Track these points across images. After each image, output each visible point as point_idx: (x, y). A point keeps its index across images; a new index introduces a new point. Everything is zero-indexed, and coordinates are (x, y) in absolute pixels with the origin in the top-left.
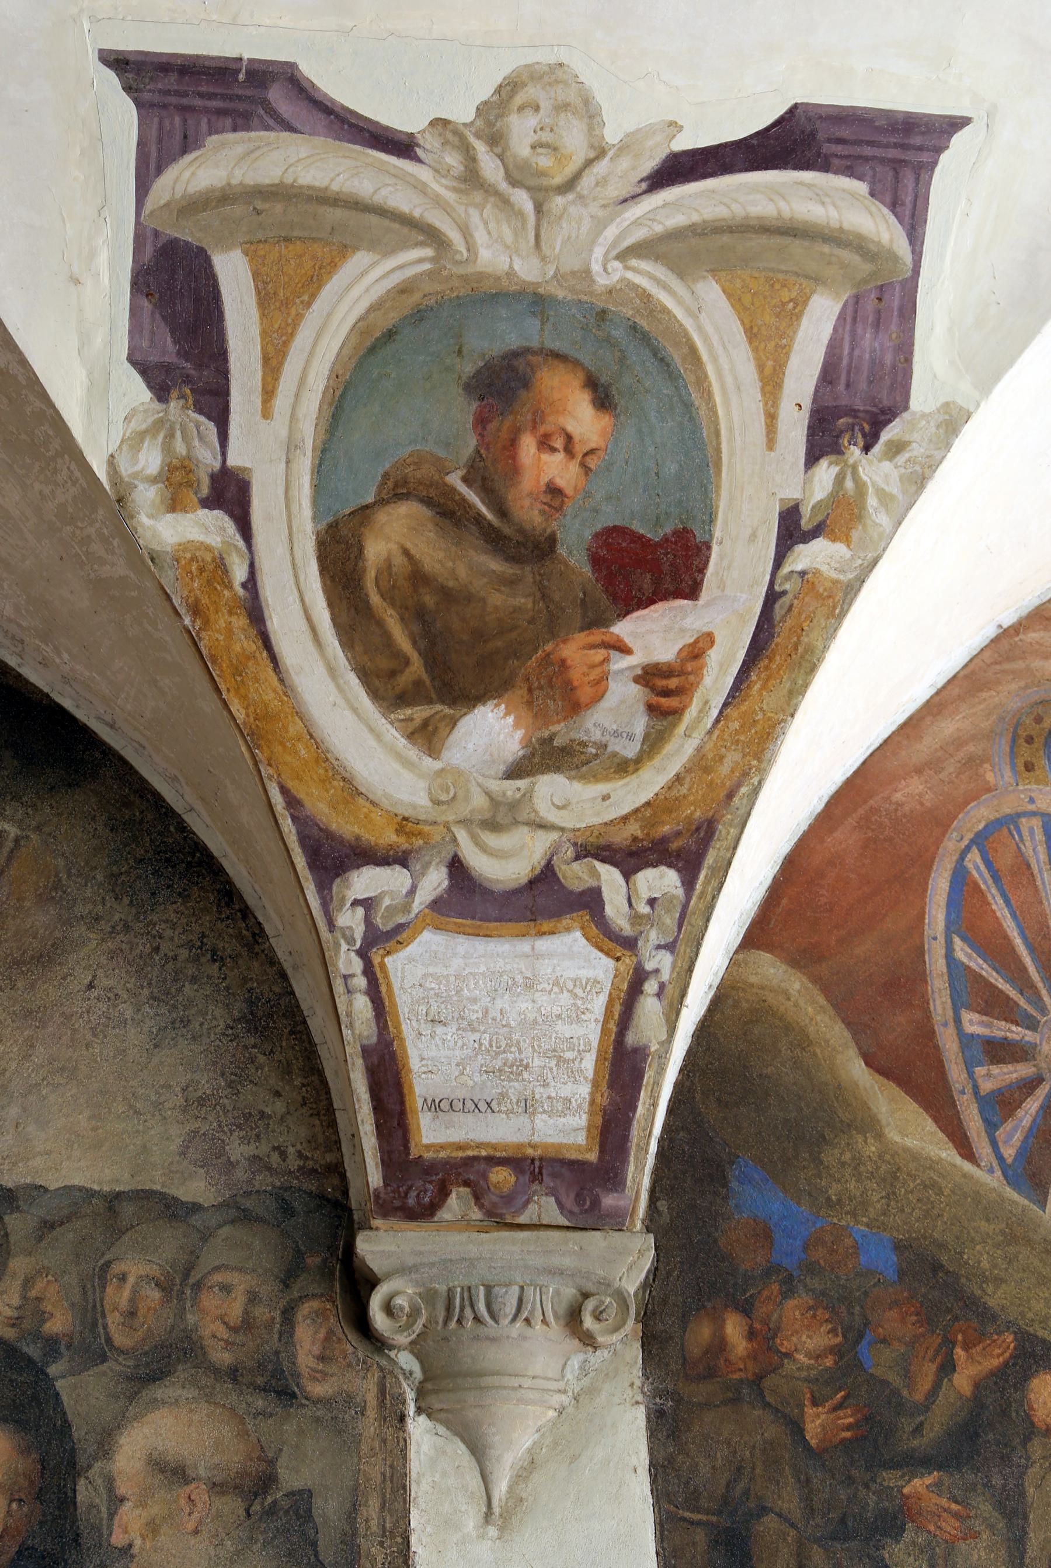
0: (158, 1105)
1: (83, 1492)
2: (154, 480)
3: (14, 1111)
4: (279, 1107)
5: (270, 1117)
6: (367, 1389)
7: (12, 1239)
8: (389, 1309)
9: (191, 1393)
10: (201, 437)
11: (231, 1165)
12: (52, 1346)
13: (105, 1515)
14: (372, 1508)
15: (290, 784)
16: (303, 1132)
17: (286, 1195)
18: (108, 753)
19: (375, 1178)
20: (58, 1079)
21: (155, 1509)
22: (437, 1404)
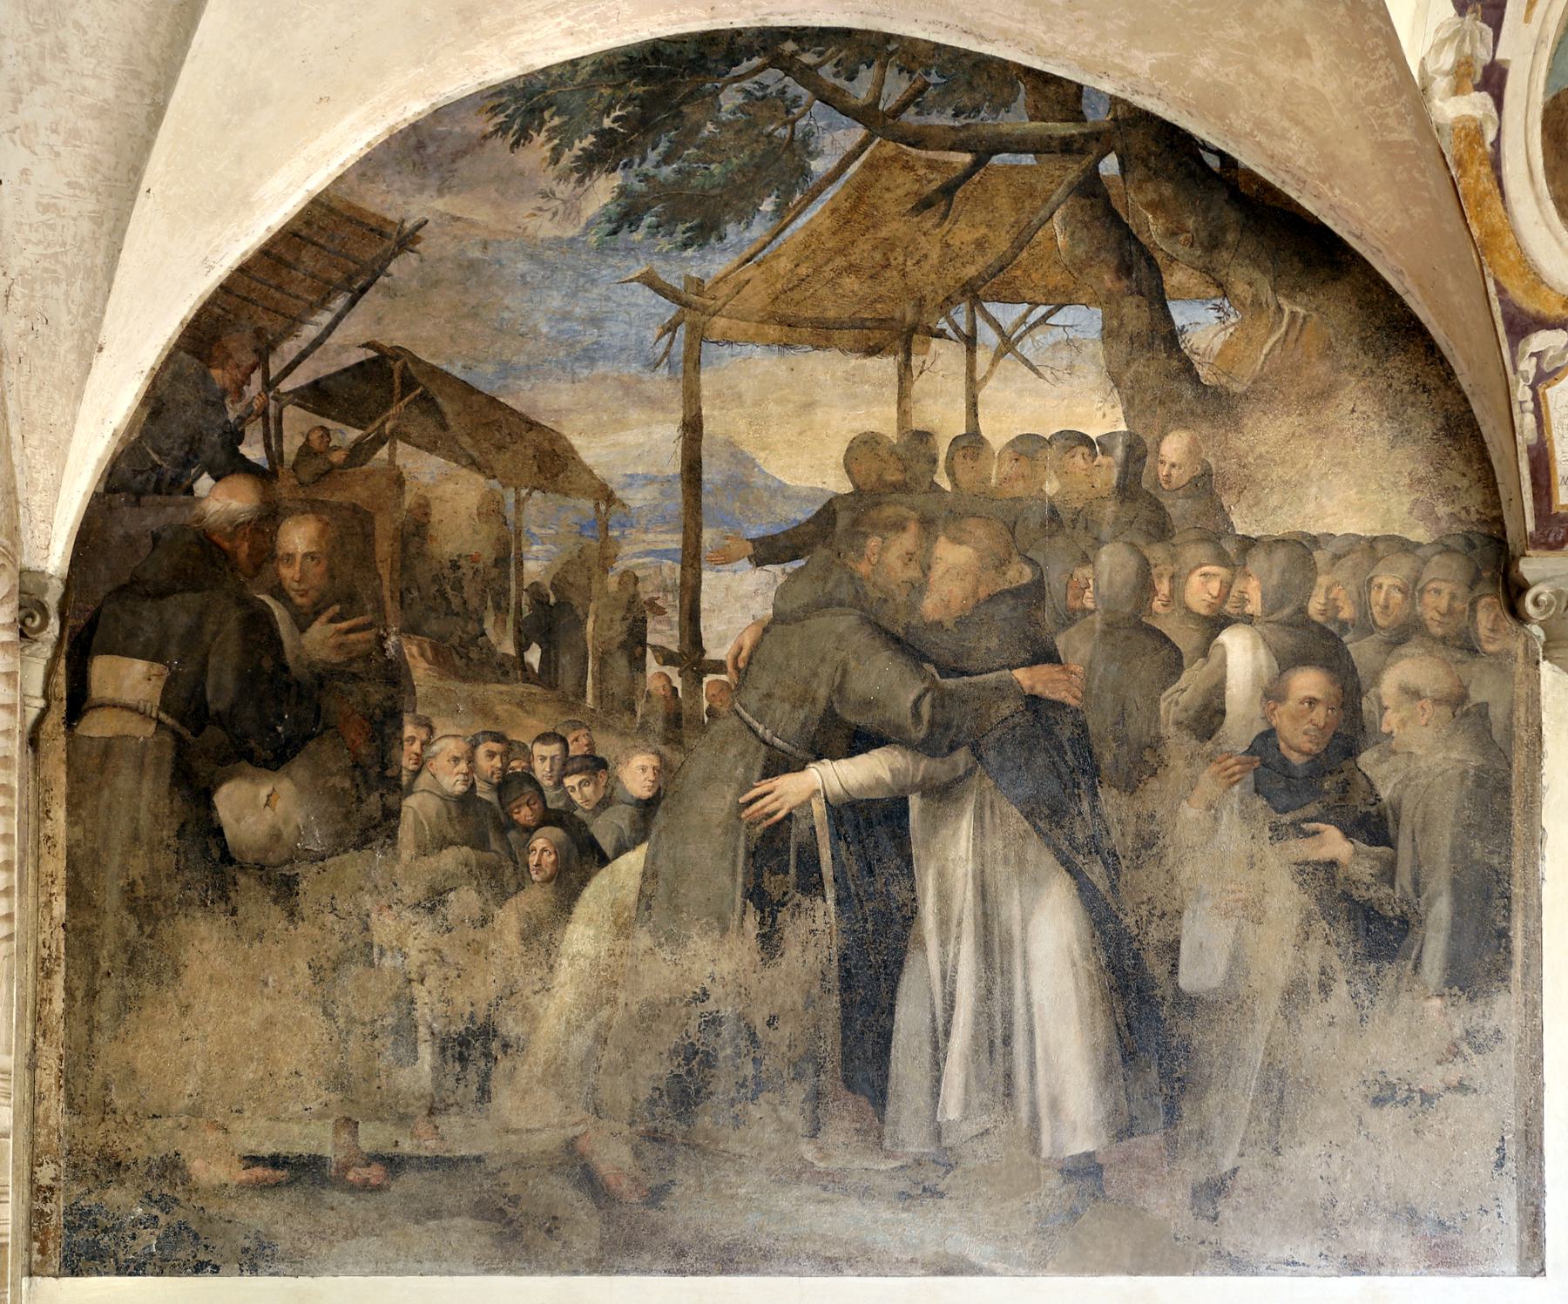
0: (1395, 484)
1: (1365, 705)
2: (1447, 74)
3: (1314, 490)
4: (1465, 483)
6: (1518, 647)
8: (1536, 602)
9: (1421, 651)
10: (1482, 40)
12: (1344, 625)
14: (1521, 712)
16: (1480, 498)
19: (1530, 526)
20: (1337, 470)
21: (1404, 713)
22: (1556, 654)
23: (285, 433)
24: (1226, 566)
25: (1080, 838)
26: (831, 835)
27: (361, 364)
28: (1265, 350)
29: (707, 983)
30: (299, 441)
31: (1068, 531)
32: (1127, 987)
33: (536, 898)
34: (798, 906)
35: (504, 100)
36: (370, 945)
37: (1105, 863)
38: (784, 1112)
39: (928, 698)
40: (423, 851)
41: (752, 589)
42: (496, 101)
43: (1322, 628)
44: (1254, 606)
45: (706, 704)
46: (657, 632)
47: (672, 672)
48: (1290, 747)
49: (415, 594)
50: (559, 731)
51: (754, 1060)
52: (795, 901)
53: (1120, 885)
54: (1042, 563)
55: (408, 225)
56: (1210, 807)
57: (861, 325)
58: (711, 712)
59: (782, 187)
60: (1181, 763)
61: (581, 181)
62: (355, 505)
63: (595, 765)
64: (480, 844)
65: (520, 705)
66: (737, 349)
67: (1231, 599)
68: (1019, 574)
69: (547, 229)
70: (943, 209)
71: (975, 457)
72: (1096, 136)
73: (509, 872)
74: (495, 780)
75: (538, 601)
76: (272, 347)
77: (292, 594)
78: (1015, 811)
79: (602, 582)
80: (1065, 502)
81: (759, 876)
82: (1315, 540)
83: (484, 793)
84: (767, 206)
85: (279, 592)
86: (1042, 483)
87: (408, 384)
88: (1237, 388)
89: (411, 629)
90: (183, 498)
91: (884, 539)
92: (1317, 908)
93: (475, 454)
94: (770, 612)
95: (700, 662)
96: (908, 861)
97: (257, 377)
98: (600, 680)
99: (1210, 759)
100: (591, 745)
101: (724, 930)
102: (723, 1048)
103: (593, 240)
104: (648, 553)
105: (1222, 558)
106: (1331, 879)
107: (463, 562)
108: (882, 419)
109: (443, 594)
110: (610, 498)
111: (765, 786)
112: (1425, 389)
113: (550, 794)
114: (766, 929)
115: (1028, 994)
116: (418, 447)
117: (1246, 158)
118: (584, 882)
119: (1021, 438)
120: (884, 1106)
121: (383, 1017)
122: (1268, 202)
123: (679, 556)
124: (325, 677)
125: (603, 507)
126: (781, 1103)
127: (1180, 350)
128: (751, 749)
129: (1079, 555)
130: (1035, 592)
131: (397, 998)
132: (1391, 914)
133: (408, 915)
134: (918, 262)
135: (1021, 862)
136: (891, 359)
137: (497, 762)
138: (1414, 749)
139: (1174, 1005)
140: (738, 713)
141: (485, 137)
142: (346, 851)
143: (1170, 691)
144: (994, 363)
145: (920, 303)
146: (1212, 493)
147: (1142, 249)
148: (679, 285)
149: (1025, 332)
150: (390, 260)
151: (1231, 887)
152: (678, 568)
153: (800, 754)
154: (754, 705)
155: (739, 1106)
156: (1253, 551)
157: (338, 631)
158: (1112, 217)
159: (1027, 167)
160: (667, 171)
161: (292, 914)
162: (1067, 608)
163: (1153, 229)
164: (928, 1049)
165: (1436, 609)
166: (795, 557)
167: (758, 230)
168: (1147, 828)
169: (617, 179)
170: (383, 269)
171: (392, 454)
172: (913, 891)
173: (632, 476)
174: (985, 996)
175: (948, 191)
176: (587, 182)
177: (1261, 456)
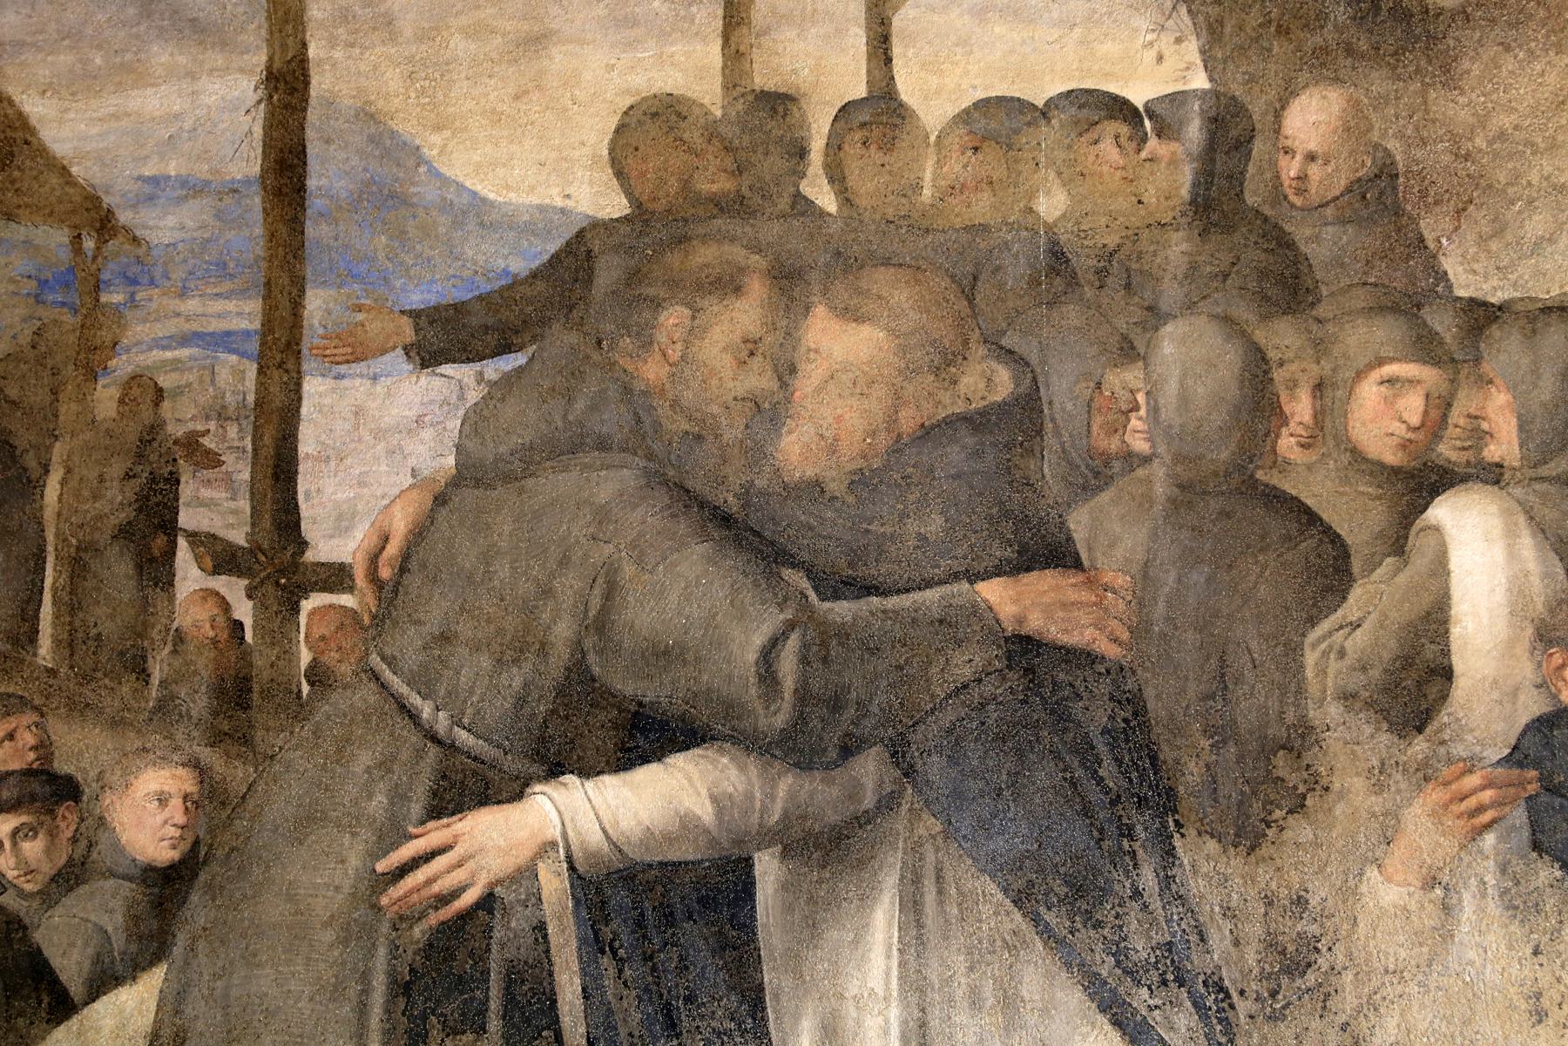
24: (1436, 362)
25: (1140, 948)
26: (582, 941)
31: (1089, 293)
37: (1198, 1006)
39: (793, 642)
41: (412, 414)
44: (1504, 446)
45: (305, 657)
46: (200, 503)
47: (233, 589)
54: (1034, 358)
56: (1431, 882)
58: (318, 675)
60: (1359, 784)
67: (1451, 431)
71: (888, 146)
78: (992, 888)
79: (82, 399)
80: (1082, 234)
86: (1031, 195)
91: (696, 312)
95: (295, 566)
96: (756, 1003)
98: (71, 606)
99: (1425, 774)
100: (44, 747)
104: (184, 340)
105: (1426, 347)
110: (105, 224)
111: (435, 835)
119: (984, 105)
123: (254, 346)
125: (89, 244)
128: (405, 755)
129: (1114, 341)
135: (1009, 1002)
140: (376, 677)
143: (1325, 626)
146: (1398, 212)
152: (252, 370)
153: (513, 764)
154: (412, 658)
156: (1495, 331)
162: (1091, 453)
166: (505, 348)
168: (1290, 929)
173: (154, 181)
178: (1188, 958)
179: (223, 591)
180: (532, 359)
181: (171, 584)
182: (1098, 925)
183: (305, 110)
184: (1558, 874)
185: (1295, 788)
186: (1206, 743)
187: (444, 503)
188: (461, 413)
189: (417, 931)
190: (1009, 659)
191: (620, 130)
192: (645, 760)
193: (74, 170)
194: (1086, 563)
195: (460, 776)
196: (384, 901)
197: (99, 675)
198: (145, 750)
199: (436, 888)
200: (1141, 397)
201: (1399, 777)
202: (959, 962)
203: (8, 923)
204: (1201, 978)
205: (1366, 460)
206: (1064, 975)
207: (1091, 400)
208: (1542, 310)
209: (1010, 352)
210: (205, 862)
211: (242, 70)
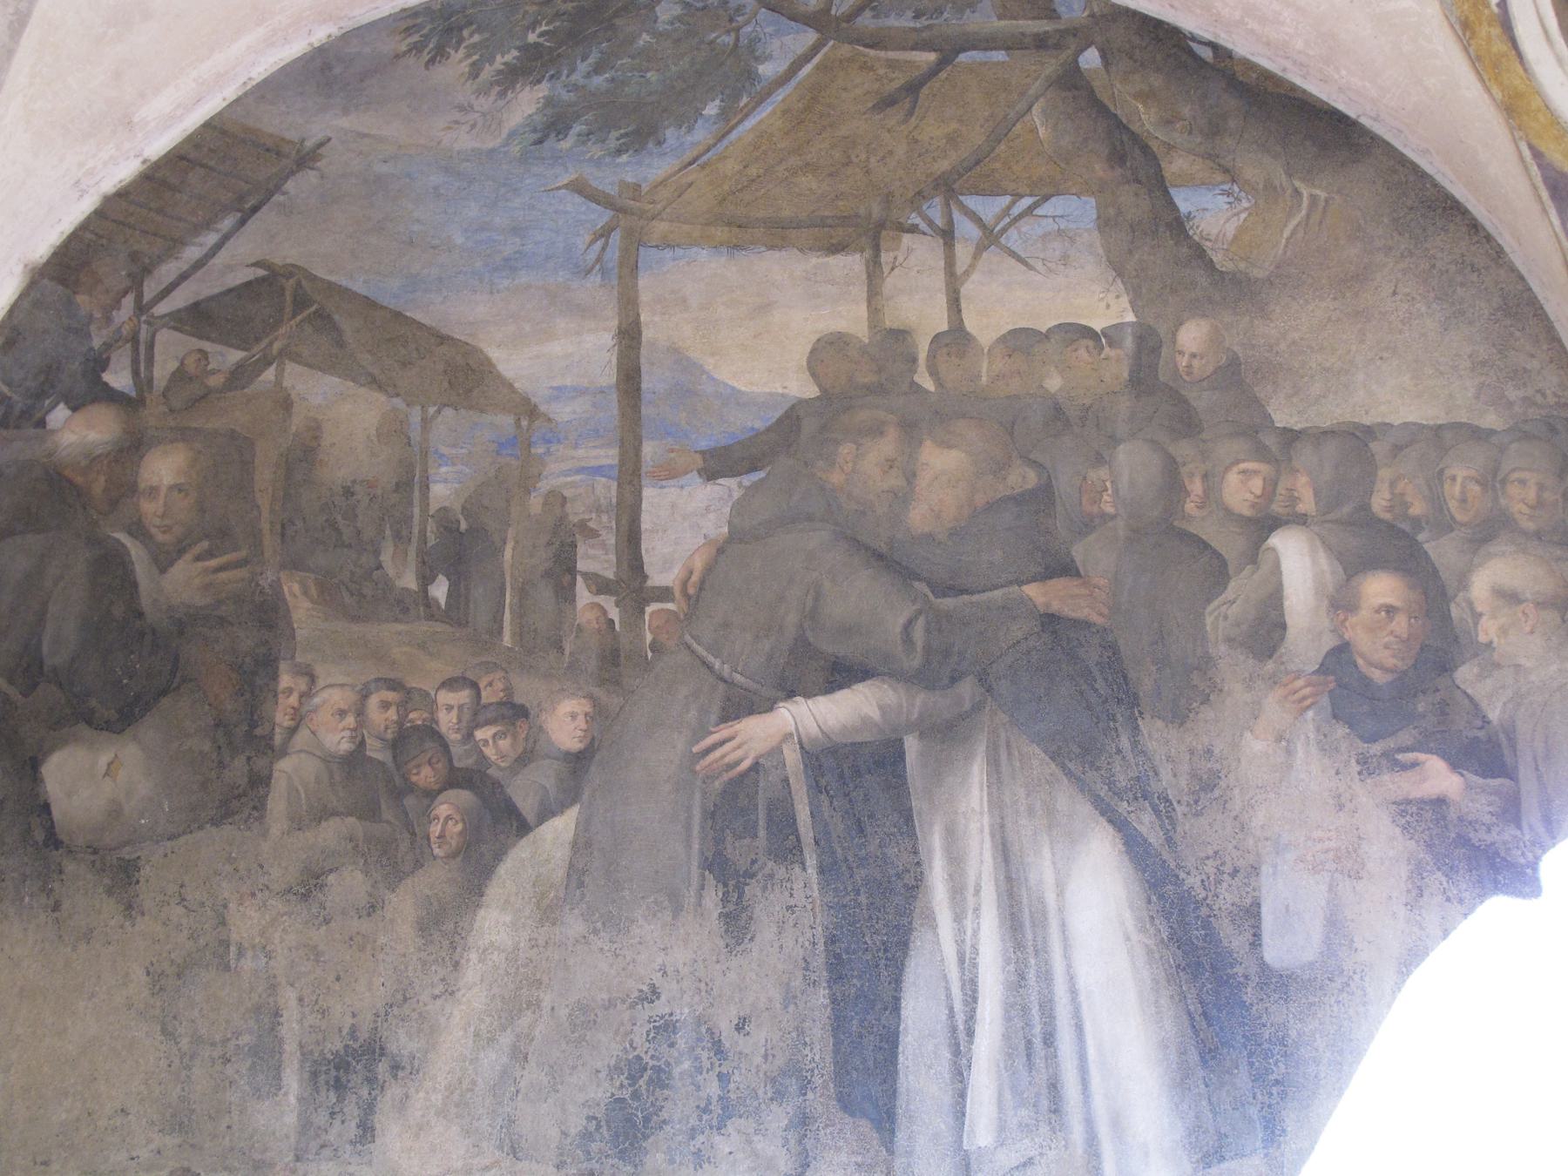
1: (1455, 612)
3: (1360, 377)
5: (1530, 371)
7: (1377, 457)
11: (1511, 404)
12: (1417, 523)
13: (1471, 625)
15: (1535, 142)
17: (1551, 421)
18: (1375, 139)
20: (1385, 355)
23: (157, 357)
24: (1269, 463)
25: (1122, 781)
26: (810, 787)
27: (248, 284)
28: (1286, 233)
29: (657, 978)
30: (173, 365)
32: (1199, 964)
33: (436, 878)
34: (771, 876)
35: (419, 20)
36: (226, 944)
37: (1156, 812)
38: (760, 1144)
39: (921, 622)
40: (298, 823)
42: (410, 22)
43: (1391, 526)
44: (1307, 504)
45: (649, 637)
47: (608, 602)
48: (1371, 664)
49: (299, 524)
50: (470, 675)
51: (720, 1076)
52: (767, 870)
53: (1177, 838)
55: (309, 144)
56: (1279, 739)
57: (822, 223)
58: (654, 647)
59: (727, 92)
61: (502, 94)
62: (233, 431)
63: (514, 713)
64: (369, 812)
65: (422, 646)
66: (679, 252)
67: (1278, 498)
68: (1022, 478)
69: (464, 141)
70: (907, 106)
72: (1074, 32)
73: (404, 846)
74: (389, 735)
75: (446, 528)
76: (147, 270)
77: (154, 531)
78: (1038, 751)
81: (719, 841)
82: (1369, 431)
83: (376, 751)
84: (711, 109)
85: (138, 530)
87: (301, 302)
88: (1257, 273)
89: (296, 564)
90: (32, 431)
91: (859, 445)
92: (1428, 858)
93: (376, 372)
94: (726, 529)
95: (641, 589)
96: (908, 817)
97: (128, 302)
98: (520, 614)
99: (1273, 681)
100: (508, 690)
101: (677, 910)
102: (678, 1062)
103: (515, 149)
105: (1261, 453)
106: (1441, 820)
107: (357, 488)
108: (851, 318)
109: (333, 525)
110: (532, 412)
111: (724, 732)
112: (1474, 269)
113: (456, 750)
114: (731, 907)
115: (1071, 978)
116: (310, 366)
117: (1241, 46)
118: (499, 856)
120: (893, 1132)
121: (237, 1035)
122: (1270, 89)
123: (615, 472)
124: (186, 623)
125: (524, 423)
126: (757, 1132)
127: (1188, 237)
130: (1042, 497)
131: (258, 1009)
132: (1522, 861)
133: (276, 904)
134: (883, 158)
135: (1050, 812)
136: (857, 256)
137: (392, 714)
138: (1522, 661)
139: (1262, 985)
140: (689, 647)
141: (397, 56)
142: (200, 828)
143: (1216, 603)
144: (976, 256)
145: (888, 199)
147: (1135, 137)
148: (612, 190)
149: (1010, 225)
150: (287, 178)
151: (1318, 834)
152: (614, 485)
155: (701, 1138)
157: (206, 571)
158: (1102, 110)
159: (998, 63)
160: (599, 81)
161: (129, 907)
163: (1146, 119)
164: (946, 1054)
165: (1523, 501)
166: (753, 469)
167: (701, 134)
169: (543, 89)
170: (278, 188)
171: (280, 373)
172: (916, 853)
173: (558, 389)
174: (1017, 982)
175: (913, 88)
176: (510, 95)
177: (1294, 342)
178: (1149, 785)
179: (602, 604)
180: (768, 474)
181: (574, 601)
182: (1098, 769)
183: (639, 349)
184: (1348, 731)
185: (1204, 690)
186: (1154, 668)
187: (723, 552)
188: (730, 504)
189: (717, 783)
190: (1043, 626)
191: (813, 351)
192: (840, 687)
193: (516, 385)
194: (1082, 573)
195: (737, 699)
196: (698, 768)
197: (537, 650)
198: (563, 690)
199: (726, 760)
200: (1108, 484)
201: (1260, 682)
202: (1022, 792)
203: (493, 784)
204: (1156, 795)
205: (1233, 514)
206: (1080, 796)
207: (1081, 485)
208: (1322, 433)
209: (1035, 462)
210: (598, 749)
211: (605, 330)
